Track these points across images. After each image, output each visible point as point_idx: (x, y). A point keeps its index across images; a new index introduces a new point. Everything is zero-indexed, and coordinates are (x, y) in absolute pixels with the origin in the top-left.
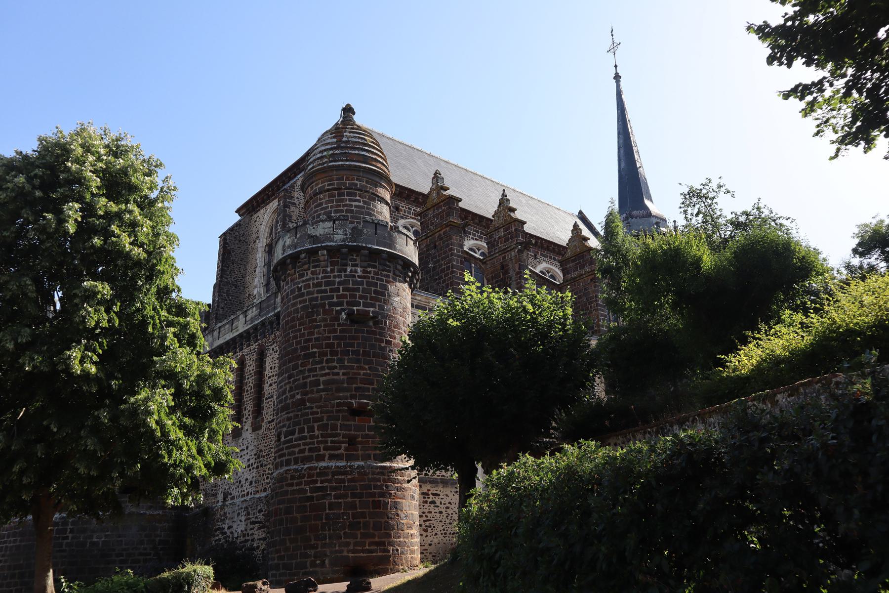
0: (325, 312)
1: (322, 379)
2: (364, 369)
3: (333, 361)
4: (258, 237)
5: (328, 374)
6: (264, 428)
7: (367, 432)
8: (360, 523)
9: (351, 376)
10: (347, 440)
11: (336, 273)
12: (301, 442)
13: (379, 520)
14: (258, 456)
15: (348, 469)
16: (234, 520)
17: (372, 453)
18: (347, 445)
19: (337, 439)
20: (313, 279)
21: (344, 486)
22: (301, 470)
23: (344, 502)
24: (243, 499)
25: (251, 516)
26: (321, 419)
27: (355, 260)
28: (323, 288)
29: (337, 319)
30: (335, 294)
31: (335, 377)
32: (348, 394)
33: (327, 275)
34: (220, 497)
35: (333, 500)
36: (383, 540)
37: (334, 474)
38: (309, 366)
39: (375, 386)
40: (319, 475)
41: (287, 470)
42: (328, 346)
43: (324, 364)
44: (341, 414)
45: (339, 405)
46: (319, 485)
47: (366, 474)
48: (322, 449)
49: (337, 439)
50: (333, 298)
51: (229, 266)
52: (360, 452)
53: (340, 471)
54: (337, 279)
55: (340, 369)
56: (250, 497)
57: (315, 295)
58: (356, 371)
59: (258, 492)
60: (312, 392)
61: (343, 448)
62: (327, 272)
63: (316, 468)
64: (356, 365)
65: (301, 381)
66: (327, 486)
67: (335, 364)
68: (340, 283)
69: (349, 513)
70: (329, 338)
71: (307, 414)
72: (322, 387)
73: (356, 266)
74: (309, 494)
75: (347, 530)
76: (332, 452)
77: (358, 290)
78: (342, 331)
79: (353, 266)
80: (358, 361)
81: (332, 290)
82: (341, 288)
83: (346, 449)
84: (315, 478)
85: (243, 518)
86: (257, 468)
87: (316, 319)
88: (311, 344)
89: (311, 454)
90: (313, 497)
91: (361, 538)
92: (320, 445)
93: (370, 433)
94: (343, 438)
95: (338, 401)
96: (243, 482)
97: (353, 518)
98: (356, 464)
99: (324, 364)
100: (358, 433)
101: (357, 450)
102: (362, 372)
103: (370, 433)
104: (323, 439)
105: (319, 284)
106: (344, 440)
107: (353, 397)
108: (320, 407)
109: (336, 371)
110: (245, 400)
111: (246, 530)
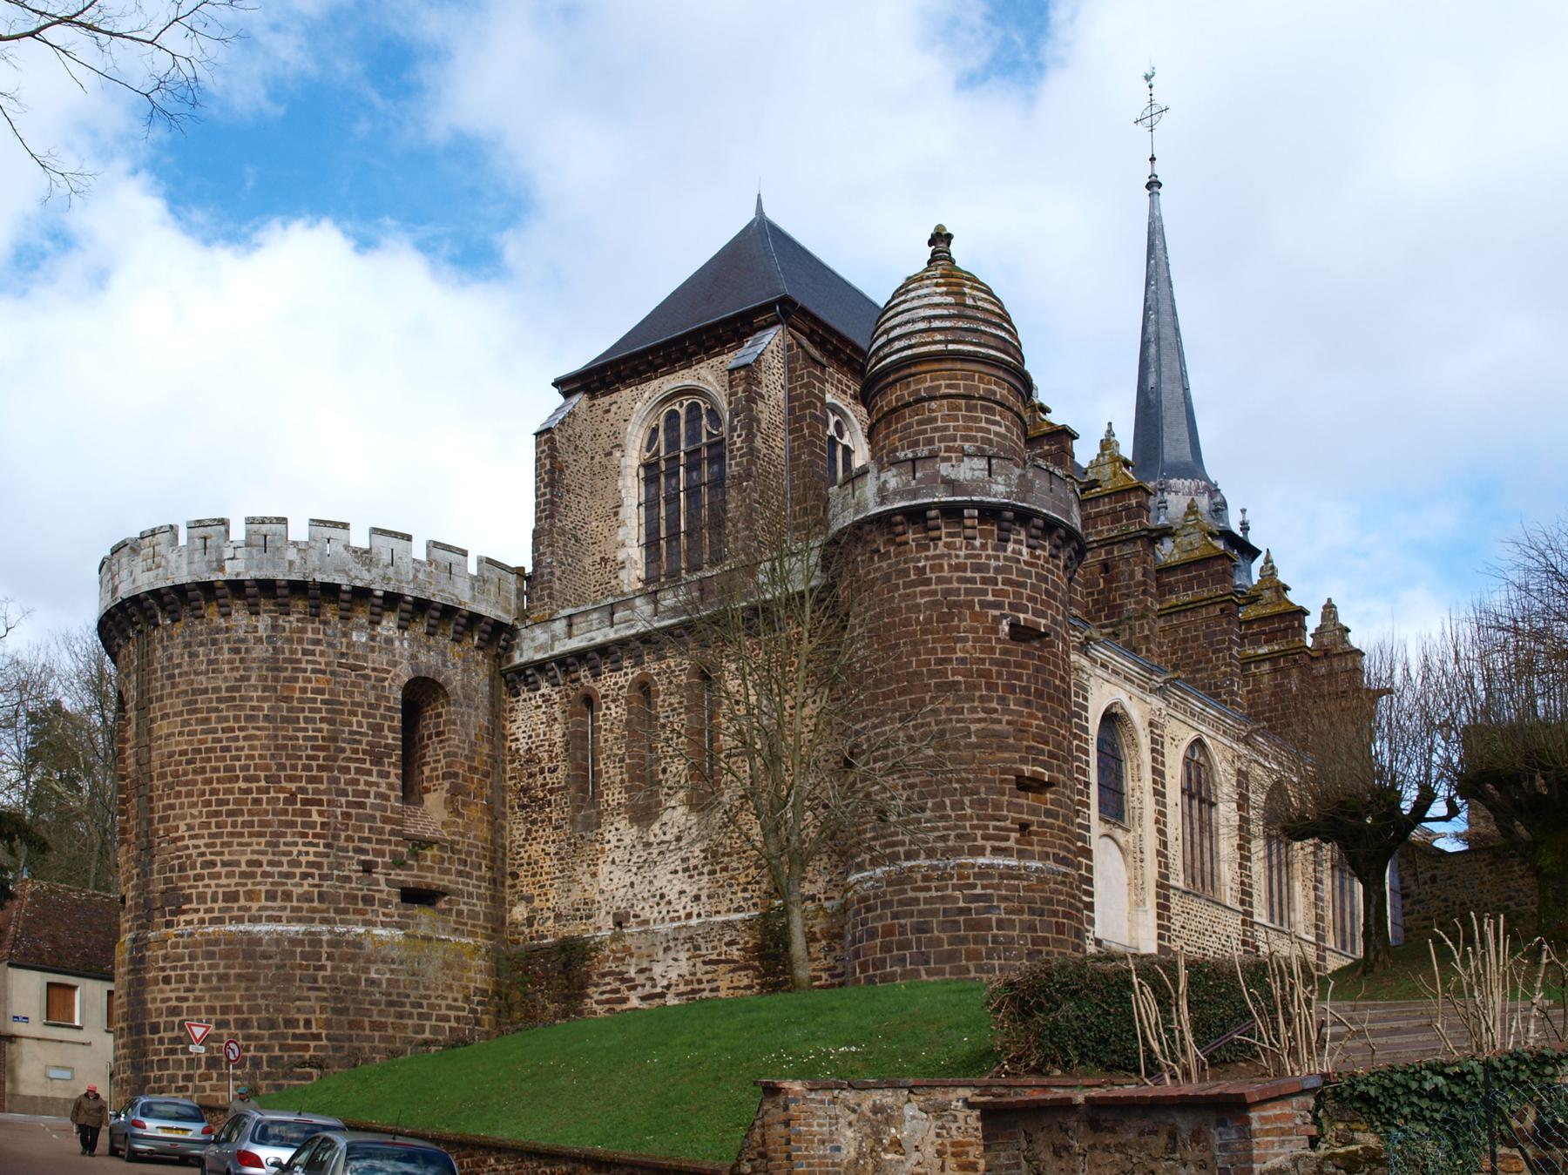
1: (973, 727)
2: (1037, 718)
7: (1043, 819)
11: (990, 552)
16: (655, 958)
19: (1002, 824)
23: (1020, 921)
24: (675, 924)
28: (969, 574)
29: (995, 631)
30: (990, 588)
32: (1017, 756)
35: (1003, 916)
37: (1001, 876)
40: (977, 876)
43: (976, 704)
45: (1004, 771)
46: (978, 891)
47: (1046, 882)
48: (979, 838)
49: (1002, 824)
52: (1037, 849)
53: (1009, 874)
55: (1003, 714)
56: (694, 922)
59: (719, 912)
61: (1012, 839)
62: (974, 548)
63: (973, 866)
67: (994, 705)
68: (997, 570)
70: (983, 661)
72: (974, 739)
76: (997, 844)
80: (1028, 704)
81: (984, 581)
82: (1000, 578)
87: (958, 627)
90: (970, 909)
96: (673, 896)
98: (1035, 864)
100: (1033, 818)
101: (1032, 845)
102: (1035, 722)
105: (960, 567)
107: (1024, 761)
109: (995, 716)
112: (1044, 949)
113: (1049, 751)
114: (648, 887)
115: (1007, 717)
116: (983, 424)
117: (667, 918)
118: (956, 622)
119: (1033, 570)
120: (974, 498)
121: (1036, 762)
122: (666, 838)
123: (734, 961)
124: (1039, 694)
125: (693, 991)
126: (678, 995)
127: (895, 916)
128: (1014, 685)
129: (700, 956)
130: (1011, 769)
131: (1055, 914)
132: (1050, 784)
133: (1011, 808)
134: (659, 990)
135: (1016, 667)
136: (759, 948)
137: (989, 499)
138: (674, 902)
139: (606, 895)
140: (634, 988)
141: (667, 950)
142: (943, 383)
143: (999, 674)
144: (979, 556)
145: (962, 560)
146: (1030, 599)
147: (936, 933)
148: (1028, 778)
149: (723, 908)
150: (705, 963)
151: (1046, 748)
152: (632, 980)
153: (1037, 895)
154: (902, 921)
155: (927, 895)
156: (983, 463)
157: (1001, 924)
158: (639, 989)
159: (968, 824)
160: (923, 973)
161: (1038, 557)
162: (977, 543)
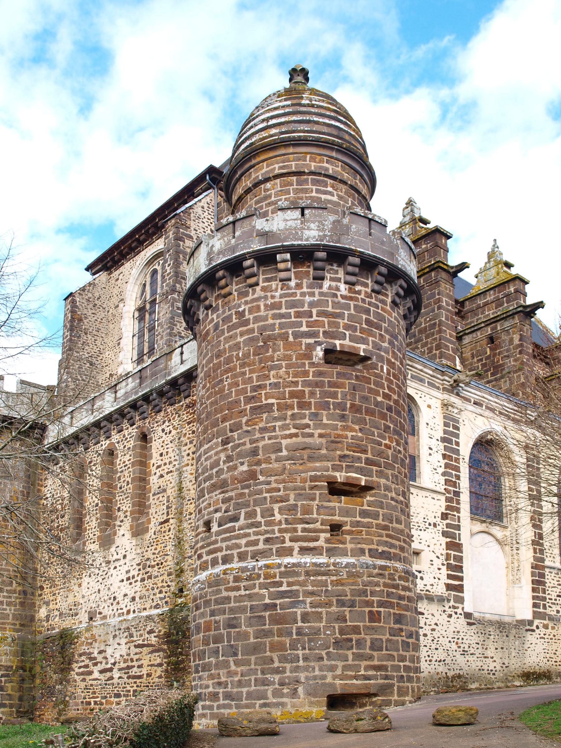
0: (288, 346)
3: (303, 417)
4: (122, 300)
5: (296, 435)
6: (151, 532)
8: (351, 640)
9: (333, 438)
10: (329, 527)
11: (305, 290)
12: (250, 531)
13: (378, 637)
14: (143, 565)
15: (332, 568)
17: (366, 547)
18: (328, 535)
19: (311, 526)
20: (266, 298)
21: (327, 591)
22: (254, 568)
23: (327, 613)
25: (135, 639)
27: (337, 272)
28: (283, 311)
30: (304, 321)
31: (308, 440)
32: (329, 464)
33: (290, 291)
34: (84, 617)
35: (309, 610)
36: (385, 663)
37: (308, 574)
38: (262, 425)
39: (370, 456)
41: (227, 569)
43: (288, 421)
44: (318, 493)
45: (314, 479)
46: (284, 588)
48: (287, 539)
49: (311, 526)
50: (302, 326)
51: (80, 336)
54: (308, 299)
55: (315, 429)
56: (131, 616)
57: (270, 321)
58: (341, 433)
59: (145, 609)
60: (268, 461)
62: (289, 288)
63: (279, 565)
64: (340, 424)
65: (248, 446)
66: (297, 590)
67: (307, 421)
68: (312, 304)
69: (334, 627)
70: (296, 383)
71: (260, 492)
72: (285, 453)
73: (339, 280)
74: (267, 601)
75: (331, 650)
76: (305, 544)
77: (340, 316)
79: (332, 279)
81: (298, 315)
82: (314, 311)
83: (327, 541)
84: (278, 579)
85: (123, 641)
86: (143, 580)
88: (263, 392)
89: (268, 546)
91: (353, 660)
92: (285, 535)
93: (362, 520)
94: (322, 524)
95: (313, 473)
97: (341, 633)
99: (288, 421)
103: (362, 520)
104: (290, 526)
105: (276, 306)
106: (324, 527)
107: (336, 468)
108: (284, 481)
109: (307, 430)
110: (117, 498)
111: (128, 655)
112: (354, 637)
113: (367, 459)
114: (107, 593)
115: (319, 431)
116: (314, 194)
117: (116, 614)
118: (270, 353)
119: (352, 303)
120: (285, 244)
121: (349, 468)
122: (118, 557)
123: (152, 645)
124: (355, 409)
125: (129, 667)
126: (120, 670)
127: (213, 614)
128: (328, 403)
129: (133, 642)
130: (322, 476)
131: (369, 604)
132: (367, 488)
133: (322, 510)
134: (109, 666)
135: (330, 386)
136: (168, 635)
137: (300, 242)
138: (121, 602)
139: (86, 599)
140: (95, 664)
141: (115, 636)
142: (277, 166)
143: (312, 394)
144: (294, 294)
145: (277, 300)
146: (347, 327)
147: (243, 627)
148: (344, 484)
149: (148, 606)
150: (136, 646)
151: (363, 456)
152: (95, 658)
153: (347, 589)
154: (217, 618)
155: (237, 594)
156: (297, 214)
157: (305, 617)
158: (99, 664)
159: (276, 528)
160: (232, 664)
161: (359, 292)
162: (293, 283)
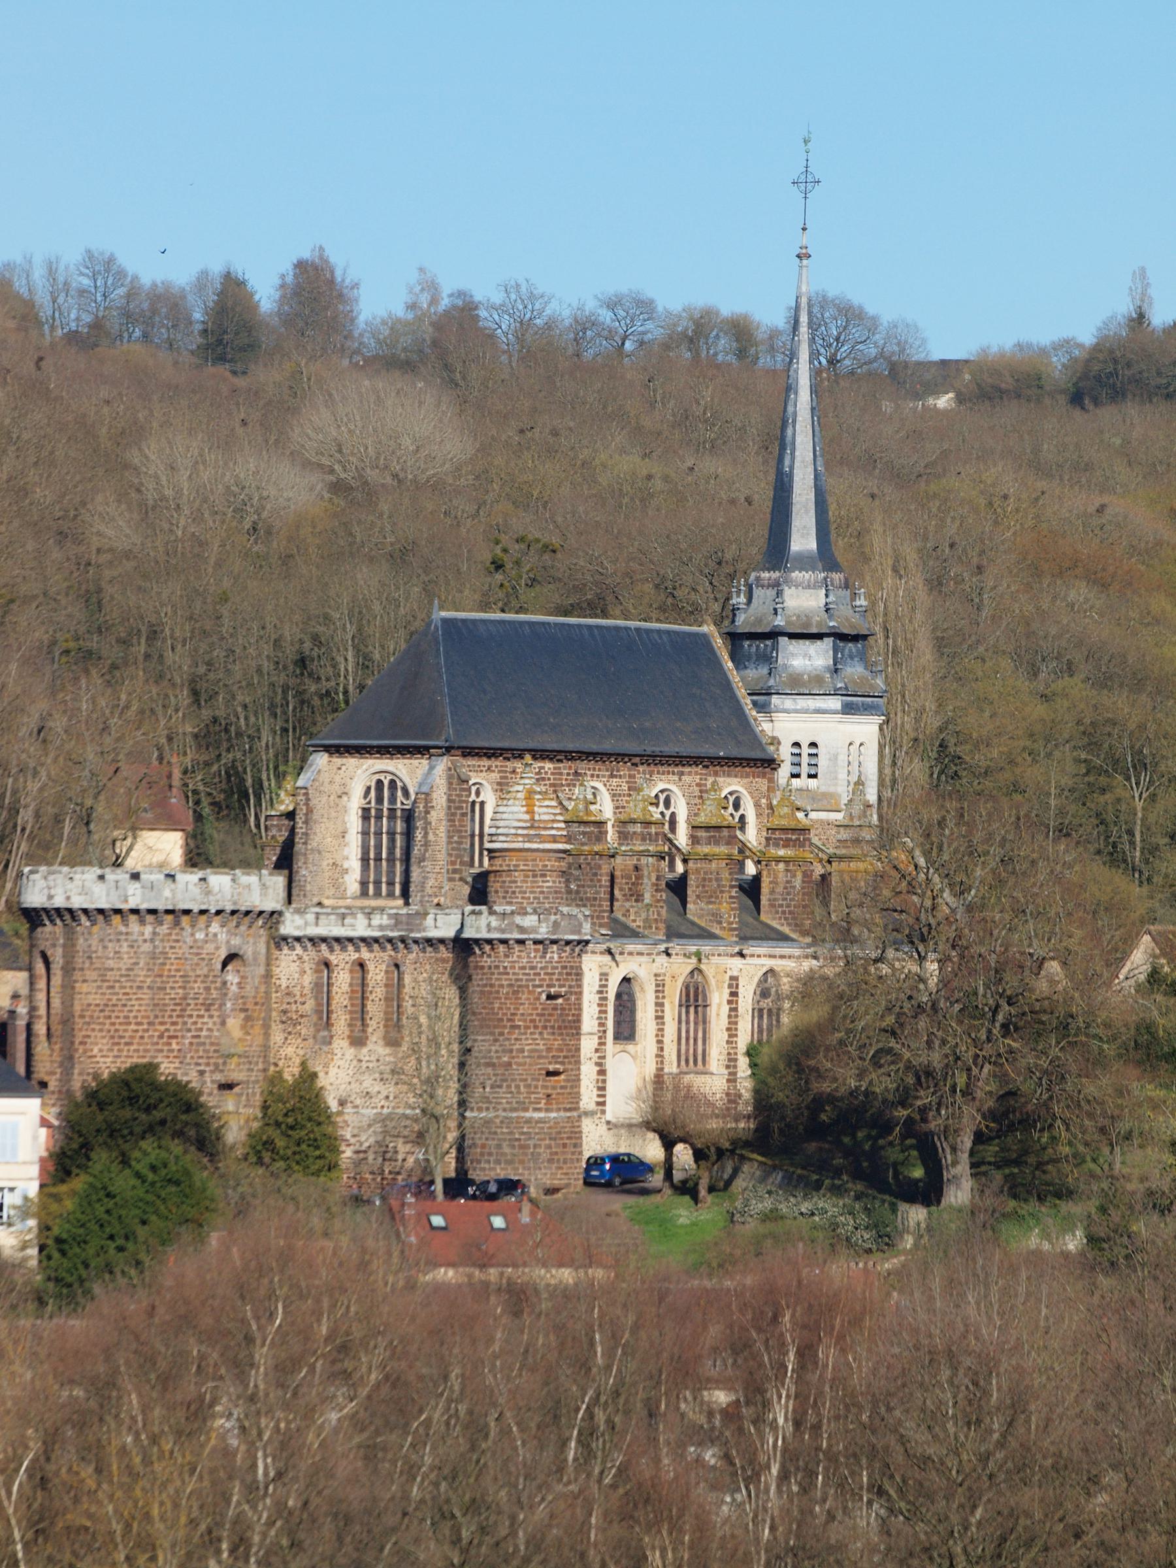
0: (530, 992)
1: (527, 1048)
26: (526, 1080)
29: (538, 999)
37: (537, 1122)
42: (531, 1021)
52: (555, 1106)
53: (540, 1121)
68: (541, 968)
78: (543, 1009)
80: (553, 1034)
81: (535, 974)
98: (553, 1115)
105: (523, 968)
107: (550, 1063)
121: (556, 1063)
